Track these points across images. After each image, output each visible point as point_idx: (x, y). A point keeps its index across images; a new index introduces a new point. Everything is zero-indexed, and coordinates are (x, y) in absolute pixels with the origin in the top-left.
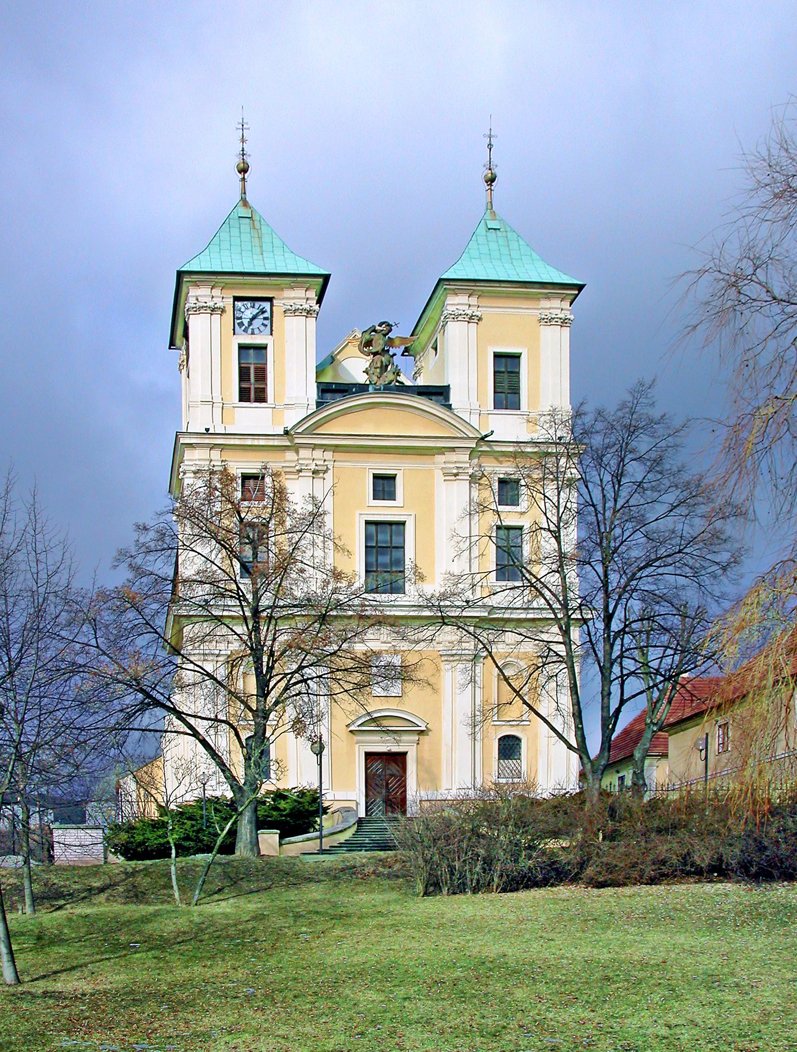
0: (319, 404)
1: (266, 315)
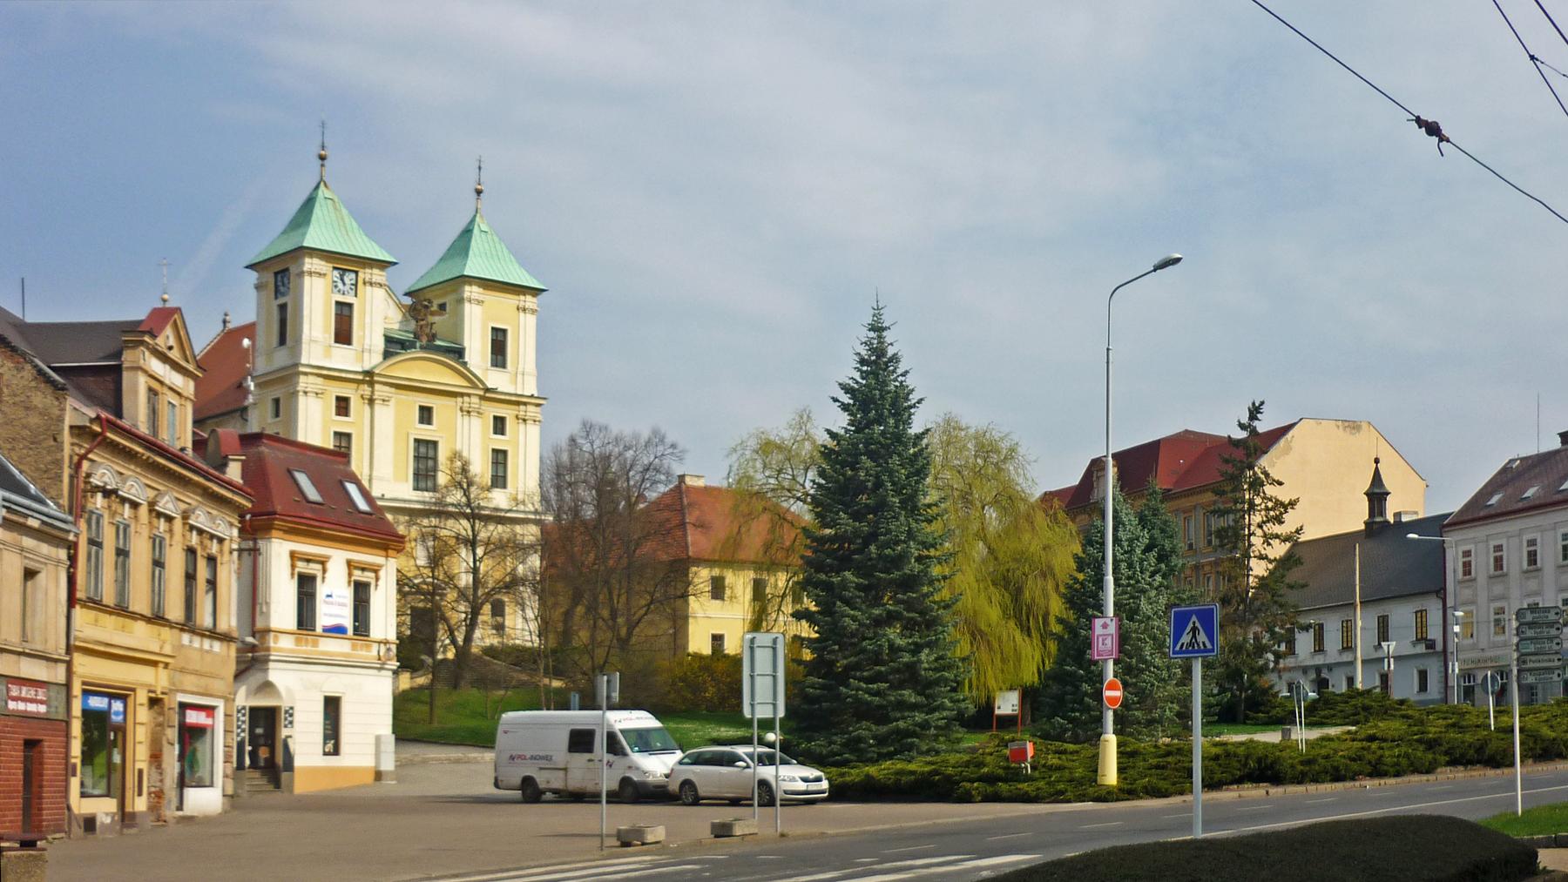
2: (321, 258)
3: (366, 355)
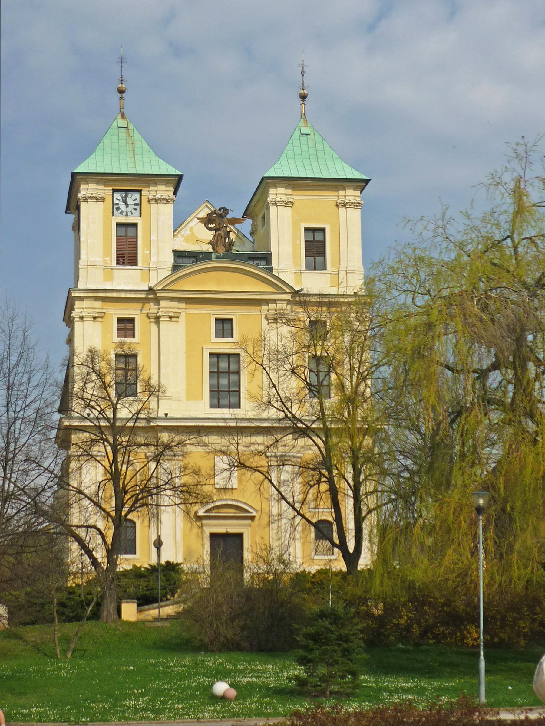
0: (175, 268)
1: (136, 202)
2: (98, 183)
3: (153, 273)
